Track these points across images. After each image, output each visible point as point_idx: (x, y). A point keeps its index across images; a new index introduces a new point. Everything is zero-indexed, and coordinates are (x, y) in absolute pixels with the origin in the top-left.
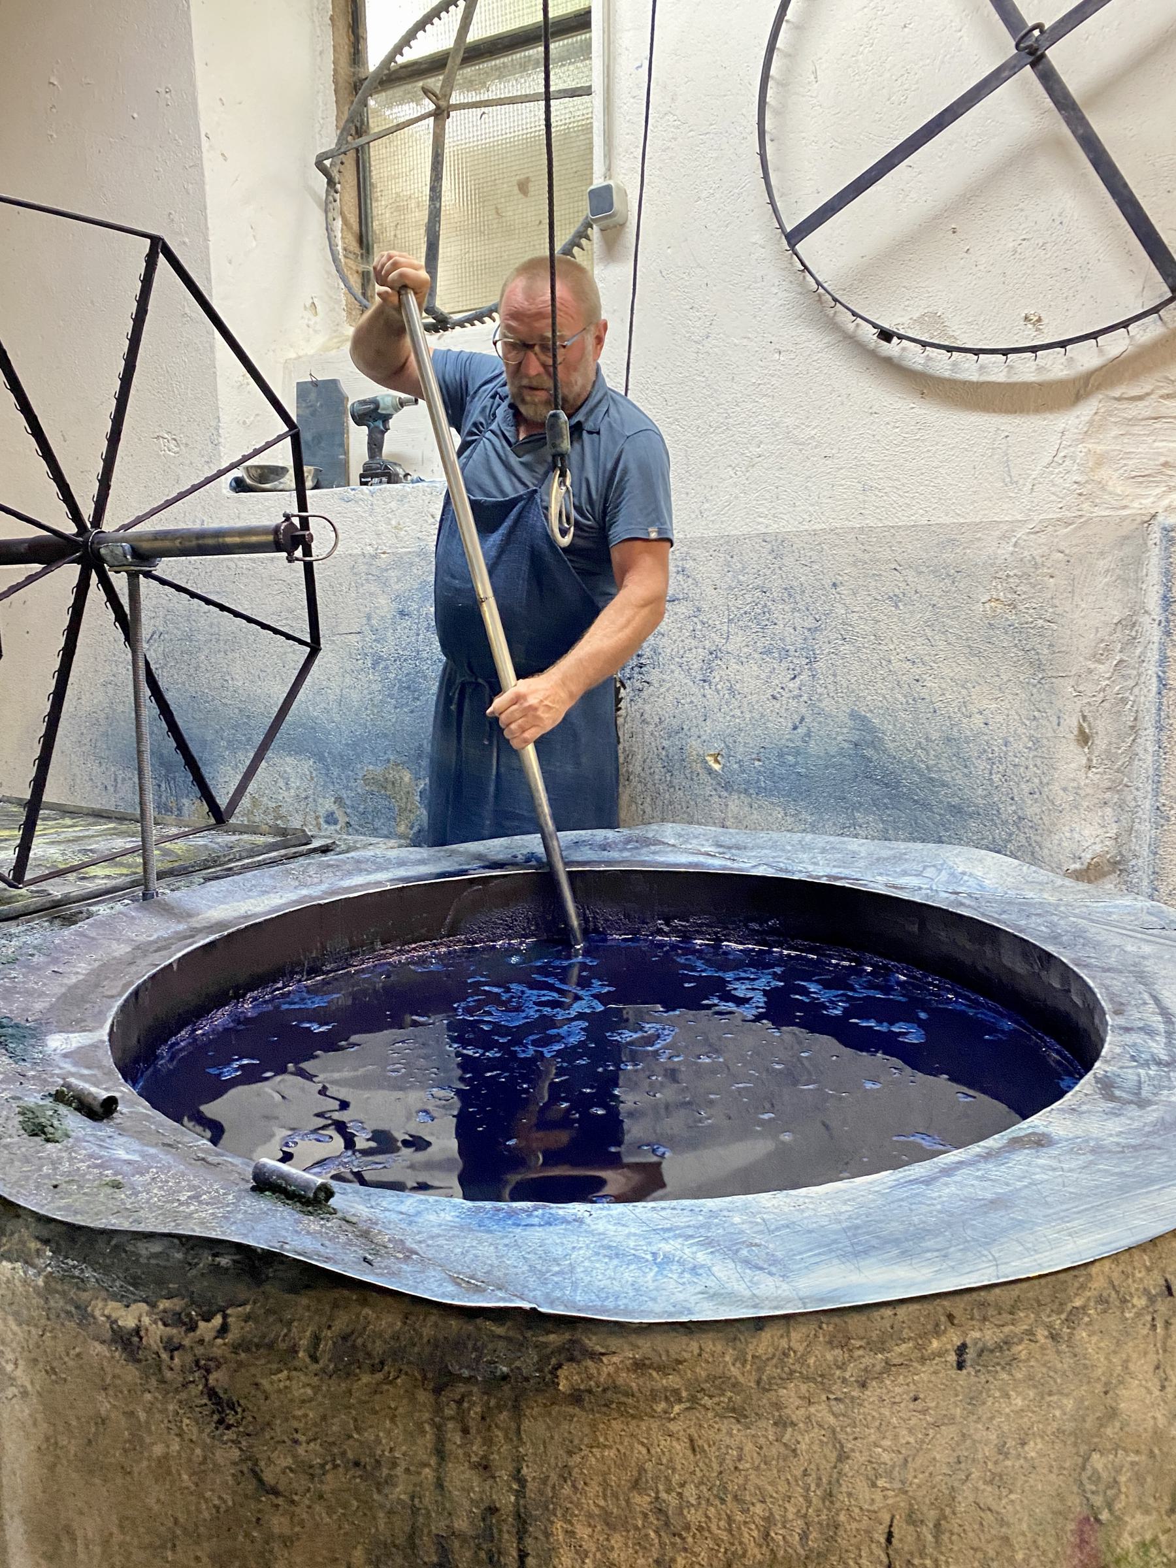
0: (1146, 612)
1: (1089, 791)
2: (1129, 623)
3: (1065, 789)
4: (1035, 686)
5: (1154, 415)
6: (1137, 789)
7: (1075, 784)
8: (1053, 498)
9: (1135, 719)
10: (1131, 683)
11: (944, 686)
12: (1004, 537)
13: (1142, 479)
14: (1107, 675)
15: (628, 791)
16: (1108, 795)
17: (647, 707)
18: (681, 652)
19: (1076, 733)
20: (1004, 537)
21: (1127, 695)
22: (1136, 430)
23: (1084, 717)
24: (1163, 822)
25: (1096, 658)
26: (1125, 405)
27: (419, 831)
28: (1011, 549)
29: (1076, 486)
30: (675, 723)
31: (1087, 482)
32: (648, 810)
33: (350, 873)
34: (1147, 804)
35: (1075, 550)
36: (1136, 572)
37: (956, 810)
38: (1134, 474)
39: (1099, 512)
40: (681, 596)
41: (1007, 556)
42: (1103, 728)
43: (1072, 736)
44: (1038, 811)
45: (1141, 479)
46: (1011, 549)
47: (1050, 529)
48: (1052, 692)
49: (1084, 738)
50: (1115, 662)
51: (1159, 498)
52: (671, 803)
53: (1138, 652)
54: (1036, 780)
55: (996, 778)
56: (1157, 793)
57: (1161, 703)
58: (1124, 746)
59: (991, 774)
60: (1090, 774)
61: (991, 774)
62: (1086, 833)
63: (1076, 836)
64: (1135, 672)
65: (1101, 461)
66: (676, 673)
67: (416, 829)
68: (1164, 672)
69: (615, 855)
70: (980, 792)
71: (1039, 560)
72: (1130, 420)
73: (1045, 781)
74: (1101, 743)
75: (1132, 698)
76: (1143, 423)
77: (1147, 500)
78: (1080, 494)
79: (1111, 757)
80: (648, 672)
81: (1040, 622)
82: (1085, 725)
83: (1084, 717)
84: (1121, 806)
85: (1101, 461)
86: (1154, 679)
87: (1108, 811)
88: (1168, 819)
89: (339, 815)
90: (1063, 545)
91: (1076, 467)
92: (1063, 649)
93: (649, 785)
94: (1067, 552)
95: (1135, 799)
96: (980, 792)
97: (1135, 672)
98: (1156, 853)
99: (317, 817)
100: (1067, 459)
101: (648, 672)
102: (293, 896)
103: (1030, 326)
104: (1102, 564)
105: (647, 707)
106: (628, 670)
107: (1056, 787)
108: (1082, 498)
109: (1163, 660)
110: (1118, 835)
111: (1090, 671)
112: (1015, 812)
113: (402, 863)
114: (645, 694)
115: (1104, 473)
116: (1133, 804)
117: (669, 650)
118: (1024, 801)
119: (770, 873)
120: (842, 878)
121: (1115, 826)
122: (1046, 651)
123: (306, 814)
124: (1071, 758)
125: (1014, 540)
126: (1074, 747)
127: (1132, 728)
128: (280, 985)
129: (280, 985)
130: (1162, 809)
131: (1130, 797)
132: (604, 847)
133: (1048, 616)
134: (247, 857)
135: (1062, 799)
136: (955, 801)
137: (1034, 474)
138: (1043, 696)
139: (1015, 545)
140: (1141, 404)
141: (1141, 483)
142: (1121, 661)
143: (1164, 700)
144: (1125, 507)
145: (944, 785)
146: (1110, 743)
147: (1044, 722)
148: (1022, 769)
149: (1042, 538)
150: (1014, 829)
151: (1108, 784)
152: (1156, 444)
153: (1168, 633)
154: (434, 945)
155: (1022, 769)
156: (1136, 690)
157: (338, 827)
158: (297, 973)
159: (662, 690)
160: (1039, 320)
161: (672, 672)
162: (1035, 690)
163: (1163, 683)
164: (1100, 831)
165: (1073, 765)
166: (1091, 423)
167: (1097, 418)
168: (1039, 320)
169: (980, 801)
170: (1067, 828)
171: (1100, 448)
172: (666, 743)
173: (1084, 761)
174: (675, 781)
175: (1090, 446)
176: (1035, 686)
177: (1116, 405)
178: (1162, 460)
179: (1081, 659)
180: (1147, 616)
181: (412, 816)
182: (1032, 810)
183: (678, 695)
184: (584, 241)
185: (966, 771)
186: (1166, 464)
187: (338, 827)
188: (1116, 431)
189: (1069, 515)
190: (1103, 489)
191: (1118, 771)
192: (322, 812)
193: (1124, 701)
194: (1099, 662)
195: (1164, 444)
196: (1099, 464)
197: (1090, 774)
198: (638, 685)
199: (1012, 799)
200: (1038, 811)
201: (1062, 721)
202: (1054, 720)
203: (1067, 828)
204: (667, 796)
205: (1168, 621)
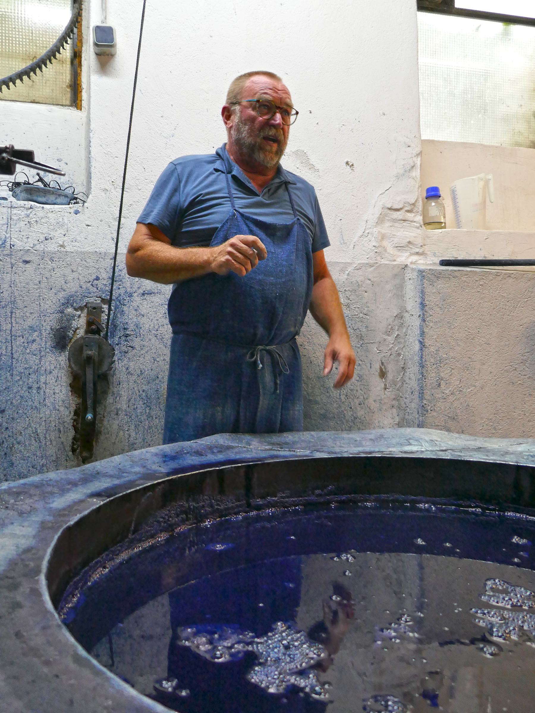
0: (406, 311)
1: (386, 401)
2: (400, 316)
3: (375, 401)
4: (359, 348)
5: (404, 219)
6: (406, 398)
7: (380, 398)
8: (364, 253)
9: (404, 364)
10: (402, 346)
11: (315, 348)
12: (342, 271)
13: (400, 248)
14: (392, 342)
15: (116, 422)
16: (394, 402)
17: (131, 364)
18: (156, 327)
19: (379, 371)
20: (342, 271)
21: (400, 352)
22: (396, 224)
23: (382, 363)
24: (425, 413)
25: (388, 333)
26: (392, 212)
28: (346, 277)
29: (374, 248)
30: (154, 373)
31: (379, 246)
32: (133, 434)
34: (413, 405)
35: (375, 279)
36: (401, 292)
37: (324, 417)
38: (397, 245)
39: (384, 262)
40: (156, 291)
41: (344, 280)
42: (391, 369)
43: (377, 374)
44: (363, 413)
45: (400, 248)
46: (346, 277)
47: (363, 268)
48: (367, 351)
49: (383, 374)
50: (396, 335)
51: (408, 258)
52: (150, 428)
53: (404, 330)
54: (362, 397)
55: (343, 397)
56: (421, 398)
57: (422, 354)
58: (400, 377)
59: (340, 395)
60: (386, 392)
61: (340, 395)
64: (403, 340)
65: (383, 237)
66: (153, 340)
68: (423, 339)
70: (335, 405)
71: (360, 283)
72: (394, 220)
73: (365, 397)
74: (390, 376)
75: (402, 353)
76: (399, 222)
77: (403, 258)
78: (376, 252)
79: (394, 383)
80: (132, 340)
81: (361, 315)
82: (383, 367)
83: (382, 363)
85: (383, 237)
86: (417, 342)
87: (394, 410)
88: (427, 411)
90: (370, 277)
91: (373, 239)
92: (372, 329)
93: (133, 417)
94: (372, 280)
95: (405, 404)
96: (335, 405)
97: (403, 340)
100: (369, 235)
101: (132, 340)
103: (349, 167)
104: (388, 287)
105: (131, 364)
106: (116, 339)
107: (371, 401)
108: (377, 254)
109: (422, 333)
111: (385, 340)
112: (352, 415)
114: (130, 355)
115: (385, 243)
116: (404, 406)
117: (147, 326)
118: (356, 408)
119: (325, 456)
120: (373, 452)
121: (397, 417)
122: (364, 330)
124: (377, 385)
125: (347, 272)
126: (378, 379)
127: (403, 368)
130: (425, 406)
131: (402, 403)
133: (365, 312)
135: (374, 406)
136: (322, 412)
137: (355, 240)
138: (363, 353)
139: (348, 274)
140: (398, 213)
141: (400, 250)
142: (398, 335)
143: (424, 353)
144: (395, 260)
145: (317, 403)
146: (394, 376)
147: (364, 367)
148: (355, 392)
149: (360, 272)
150: (352, 424)
151: (394, 397)
152: (405, 233)
153: (424, 321)
155: (355, 392)
156: (404, 349)
159: (142, 352)
160: (353, 165)
161: (150, 340)
162: (359, 350)
163: (422, 344)
164: (391, 421)
165: (378, 388)
166: (379, 218)
167: (381, 216)
168: (353, 165)
169: (336, 411)
170: (377, 421)
171: (383, 231)
172: (145, 388)
173: (383, 386)
174: (153, 413)
175: (379, 229)
176: (359, 348)
177: (389, 211)
178: (408, 240)
179: (381, 334)
180: (407, 313)
182: (360, 413)
183: (155, 356)
184: (32, 74)
185: (327, 394)
186: (409, 242)
188: (388, 224)
189: (372, 262)
190: (386, 251)
191: (398, 390)
193: (399, 355)
194: (389, 335)
195: (407, 233)
196: (383, 239)
197: (386, 392)
198: (124, 349)
199: (351, 408)
200: (363, 413)
201: (372, 365)
202: (369, 365)
204: (147, 422)
205: (424, 315)
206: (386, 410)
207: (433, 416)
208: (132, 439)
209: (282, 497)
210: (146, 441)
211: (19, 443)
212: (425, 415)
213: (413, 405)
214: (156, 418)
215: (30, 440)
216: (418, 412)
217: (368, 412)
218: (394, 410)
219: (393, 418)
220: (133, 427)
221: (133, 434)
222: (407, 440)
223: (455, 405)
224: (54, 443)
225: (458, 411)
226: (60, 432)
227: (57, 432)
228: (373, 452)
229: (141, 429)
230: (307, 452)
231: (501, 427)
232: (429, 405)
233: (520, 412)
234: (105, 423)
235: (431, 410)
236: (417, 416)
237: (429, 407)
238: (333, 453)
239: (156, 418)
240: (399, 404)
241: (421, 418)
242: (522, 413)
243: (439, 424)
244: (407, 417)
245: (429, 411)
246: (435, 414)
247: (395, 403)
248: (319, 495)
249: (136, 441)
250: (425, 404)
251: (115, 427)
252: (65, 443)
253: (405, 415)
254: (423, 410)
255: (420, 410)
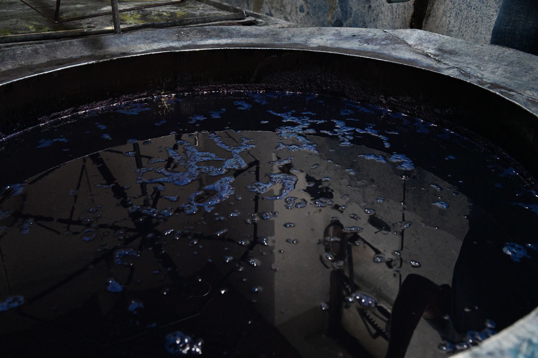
27: (337, 21)
32: (452, 21)
33: (210, 37)
67: (335, 19)
69: (370, 47)
89: (305, 7)
99: (297, 8)
102: (164, 45)
113: (244, 35)
123: (292, 5)
128: (145, 94)
129: (145, 94)
132: (368, 41)
134: (201, 23)
154: (247, 86)
157: (304, 14)
158: (158, 89)
181: (334, 12)
187: (304, 14)
192: (298, 5)
204: (465, 13)
208: (450, 26)
210: (461, 31)
211: (382, 12)
214: (474, 9)
215: (388, 11)
220: (454, 14)
221: (452, 21)
224: (400, 17)
226: (405, 8)
227: (403, 8)
229: (460, 17)
234: (435, 6)
239: (474, 9)
249: (454, 29)
251: (441, 11)
252: (407, 19)
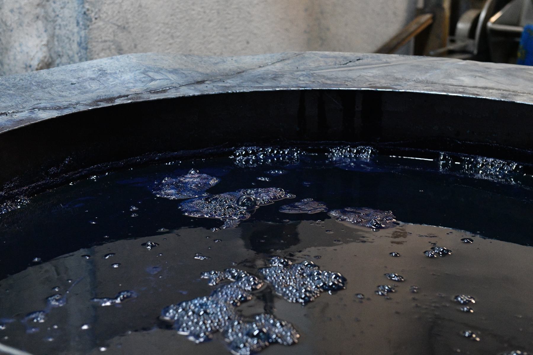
1: (27, 9)
3: (12, 11)
7: (17, 5)
24: (88, 23)
62: (30, 44)
63: (24, 48)
84: (46, 18)
87: (40, 23)
88: (91, 21)
95: (54, 11)
98: (86, 49)
110: (48, 42)
116: (53, 14)
119: (55, 114)
121: (45, 35)
130: (87, 13)
131: (50, 10)
135: (11, 19)
164: (38, 41)
203: (16, 44)
206: (29, 25)
207: (98, 27)
209: (11, 189)
212: (88, 26)
213: (67, 12)
216: (78, 23)
217: (4, 31)
218: (40, 23)
219: (39, 37)
222: (143, 73)
223: (125, 8)
225: (129, 16)
228: (115, 98)
230: (24, 115)
231: (178, 34)
232: (92, 11)
233: (199, 9)
235: (96, 19)
236: (76, 30)
237: (93, 14)
238: (59, 108)
240: (46, 12)
241: (83, 33)
242: (202, 10)
243: (107, 39)
244: (57, 32)
245: (93, 19)
246: (101, 23)
247: (40, 11)
248: (56, 175)
250: (88, 10)
253: (55, 29)
254: (86, 19)
255: (80, 19)
